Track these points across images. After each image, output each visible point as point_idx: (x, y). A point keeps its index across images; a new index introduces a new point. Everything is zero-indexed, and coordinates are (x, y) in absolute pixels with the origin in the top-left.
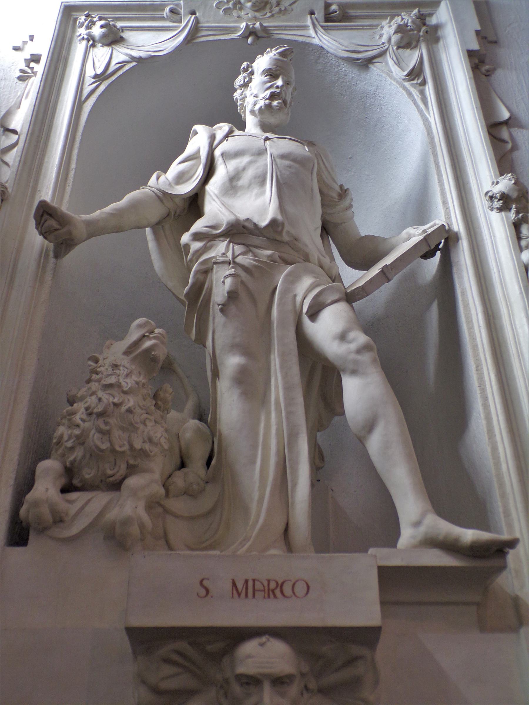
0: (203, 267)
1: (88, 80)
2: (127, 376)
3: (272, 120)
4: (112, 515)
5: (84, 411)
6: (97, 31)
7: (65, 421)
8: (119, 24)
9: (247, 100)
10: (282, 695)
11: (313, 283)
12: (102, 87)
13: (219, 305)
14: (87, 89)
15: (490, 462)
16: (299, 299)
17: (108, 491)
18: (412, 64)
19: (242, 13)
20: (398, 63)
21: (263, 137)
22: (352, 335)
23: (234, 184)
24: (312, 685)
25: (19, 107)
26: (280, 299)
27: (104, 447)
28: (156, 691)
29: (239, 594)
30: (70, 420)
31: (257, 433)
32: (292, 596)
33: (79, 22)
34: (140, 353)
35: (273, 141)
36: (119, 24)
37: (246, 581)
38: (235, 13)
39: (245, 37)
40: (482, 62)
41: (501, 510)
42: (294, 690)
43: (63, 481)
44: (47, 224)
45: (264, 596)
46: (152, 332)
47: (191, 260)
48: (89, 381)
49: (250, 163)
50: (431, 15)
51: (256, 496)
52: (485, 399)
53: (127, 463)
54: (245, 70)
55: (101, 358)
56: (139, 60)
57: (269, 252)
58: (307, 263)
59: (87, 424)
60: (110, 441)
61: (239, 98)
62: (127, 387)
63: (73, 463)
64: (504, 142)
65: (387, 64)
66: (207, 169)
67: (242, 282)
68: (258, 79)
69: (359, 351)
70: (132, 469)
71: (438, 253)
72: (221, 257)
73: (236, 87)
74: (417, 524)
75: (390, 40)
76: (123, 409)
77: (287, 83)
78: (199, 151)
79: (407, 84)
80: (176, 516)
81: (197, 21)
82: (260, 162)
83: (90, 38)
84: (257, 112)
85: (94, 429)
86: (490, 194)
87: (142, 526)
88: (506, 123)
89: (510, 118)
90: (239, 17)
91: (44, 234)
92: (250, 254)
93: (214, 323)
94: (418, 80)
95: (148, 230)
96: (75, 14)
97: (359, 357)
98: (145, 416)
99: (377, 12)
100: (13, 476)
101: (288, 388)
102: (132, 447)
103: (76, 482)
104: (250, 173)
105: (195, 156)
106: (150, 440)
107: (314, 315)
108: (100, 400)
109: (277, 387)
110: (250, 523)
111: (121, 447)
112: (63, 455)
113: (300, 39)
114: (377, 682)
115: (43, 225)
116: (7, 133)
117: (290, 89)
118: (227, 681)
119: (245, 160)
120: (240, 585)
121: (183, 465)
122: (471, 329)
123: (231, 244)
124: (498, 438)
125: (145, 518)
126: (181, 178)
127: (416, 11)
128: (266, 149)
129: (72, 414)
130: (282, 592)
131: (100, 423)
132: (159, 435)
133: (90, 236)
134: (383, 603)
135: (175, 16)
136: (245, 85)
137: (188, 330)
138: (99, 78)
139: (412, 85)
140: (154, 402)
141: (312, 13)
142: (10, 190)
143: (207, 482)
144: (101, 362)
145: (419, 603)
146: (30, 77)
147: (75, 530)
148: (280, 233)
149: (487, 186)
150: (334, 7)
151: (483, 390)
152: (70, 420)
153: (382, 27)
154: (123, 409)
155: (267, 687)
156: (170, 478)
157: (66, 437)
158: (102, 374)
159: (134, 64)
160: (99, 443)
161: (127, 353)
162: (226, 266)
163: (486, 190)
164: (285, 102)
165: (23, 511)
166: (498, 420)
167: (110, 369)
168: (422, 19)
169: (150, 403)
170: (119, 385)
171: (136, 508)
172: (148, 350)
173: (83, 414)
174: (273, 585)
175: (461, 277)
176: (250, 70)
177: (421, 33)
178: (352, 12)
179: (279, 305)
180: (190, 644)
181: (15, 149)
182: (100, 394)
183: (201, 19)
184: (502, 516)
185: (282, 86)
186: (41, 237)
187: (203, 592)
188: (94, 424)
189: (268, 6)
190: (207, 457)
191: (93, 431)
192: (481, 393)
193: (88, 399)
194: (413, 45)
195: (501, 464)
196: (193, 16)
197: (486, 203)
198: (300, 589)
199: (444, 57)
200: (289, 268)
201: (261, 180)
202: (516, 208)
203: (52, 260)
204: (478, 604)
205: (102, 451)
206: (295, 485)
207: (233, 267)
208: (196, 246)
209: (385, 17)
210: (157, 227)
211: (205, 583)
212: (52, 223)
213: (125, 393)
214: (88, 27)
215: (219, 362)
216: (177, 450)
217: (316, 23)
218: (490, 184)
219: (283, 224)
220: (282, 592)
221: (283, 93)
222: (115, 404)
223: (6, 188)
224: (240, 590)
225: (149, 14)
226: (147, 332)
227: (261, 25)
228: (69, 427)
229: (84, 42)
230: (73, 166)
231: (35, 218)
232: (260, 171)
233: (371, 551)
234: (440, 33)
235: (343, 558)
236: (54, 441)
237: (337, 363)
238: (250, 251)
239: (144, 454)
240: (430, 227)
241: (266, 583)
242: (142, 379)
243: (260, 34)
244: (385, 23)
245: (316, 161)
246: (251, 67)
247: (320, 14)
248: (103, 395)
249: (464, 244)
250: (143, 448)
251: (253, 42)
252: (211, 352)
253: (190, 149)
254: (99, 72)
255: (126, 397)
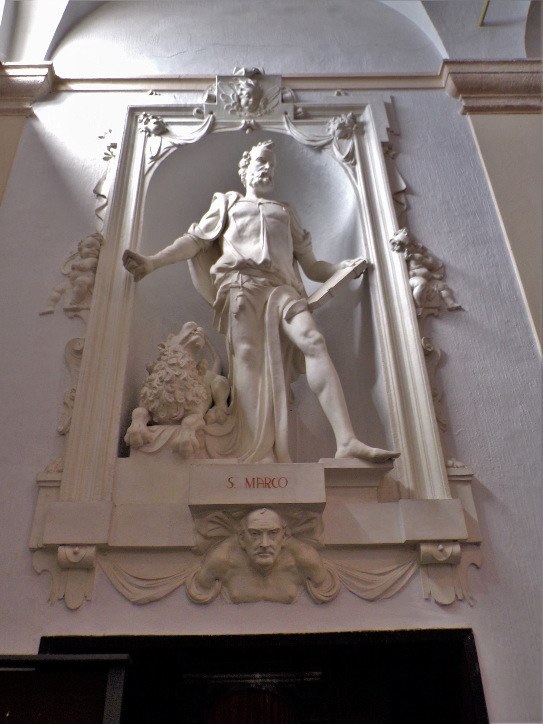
0: (225, 290)
1: (148, 160)
2: (182, 358)
3: (262, 190)
4: (177, 439)
5: (158, 379)
6: (152, 126)
7: (147, 384)
8: (166, 120)
9: (247, 176)
10: (273, 539)
11: (288, 299)
12: (157, 165)
13: (234, 313)
14: (147, 166)
15: (387, 407)
16: (280, 309)
17: (174, 425)
18: (348, 150)
19: (242, 113)
20: (340, 149)
21: (258, 203)
22: (312, 333)
23: (241, 234)
24: (289, 532)
25: (105, 179)
26: (270, 310)
27: (171, 401)
28: (206, 537)
29: (250, 486)
30: (150, 384)
31: (257, 390)
32: (278, 487)
33: (140, 120)
34: (188, 344)
35: (264, 206)
36: (166, 120)
37: (254, 479)
38: (238, 113)
39: (244, 129)
40: (390, 148)
41: (392, 434)
42: (279, 537)
43: (148, 420)
44: (131, 264)
45: (263, 487)
46: (195, 330)
47: (217, 284)
48: (159, 359)
49: (251, 221)
50: (359, 115)
51: (257, 426)
52: (386, 369)
53: (184, 409)
54: (246, 157)
55: (166, 345)
56: (179, 146)
57: (263, 279)
58: (285, 285)
59: (161, 387)
60: (174, 397)
61: (242, 175)
62: (183, 365)
63: (153, 409)
64: (402, 204)
65: (333, 150)
66: (224, 223)
67: (248, 299)
68: (254, 163)
69: (315, 343)
70: (187, 413)
71: (362, 276)
72: (235, 283)
73: (241, 167)
74: (346, 445)
75: (334, 133)
76: (182, 378)
77: (271, 166)
78: (218, 211)
79: (345, 164)
80: (211, 435)
81: (214, 118)
82: (256, 221)
83: (147, 130)
84: (253, 185)
85: (165, 390)
86: (393, 241)
87: (194, 445)
88: (404, 191)
89: (406, 189)
90: (240, 116)
91: (129, 269)
92: (252, 281)
93: (231, 324)
94: (351, 161)
95: (189, 261)
96: (137, 113)
97: (315, 347)
98: (193, 381)
99: (326, 113)
100: (119, 417)
101: (275, 364)
102: (187, 400)
103: (155, 420)
104: (250, 228)
105: (216, 214)
106: (197, 395)
107: (289, 319)
108: (168, 373)
109: (268, 362)
110: (254, 443)
111: (180, 400)
112: (147, 404)
113: (279, 131)
114: (323, 530)
115: (128, 264)
116: (99, 197)
117: (274, 169)
118: (243, 532)
119: (247, 219)
120: (250, 481)
121: (213, 404)
122: (379, 326)
123: (240, 275)
124: (392, 392)
125: (196, 441)
126: (209, 228)
127: (350, 114)
128: (259, 211)
129: (151, 380)
130: (273, 484)
131: (169, 387)
132: (201, 392)
133: (156, 268)
134: (327, 487)
135: (200, 115)
136: (246, 166)
137: (215, 325)
138: (154, 159)
139: (348, 165)
140: (198, 372)
141: (286, 113)
142: (105, 238)
143: (228, 415)
144: (166, 348)
145: (346, 487)
146: (110, 158)
147: (155, 448)
148: (269, 268)
149: (391, 236)
150: (300, 110)
151: (385, 363)
152: (150, 384)
153: (330, 124)
154: (182, 378)
155: (265, 535)
156: (207, 414)
157: (148, 394)
158: (168, 356)
159: (175, 148)
160: (168, 399)
161: (182, 343)
162: (237, 290)
163: (390, 238)
164: (270, 179)
165: (126, 438)
166: (393, 381)
167: (172, 354)
168: (354, 119)
169: (196, 372)
170: (178, 364)
171: (190, 435)
172: (194, 342)
173: (158, 381)
174: (268, 481)
175: (374, 294)
176: (249, 157)
177: (354, 129)
178: (311, 113)
179: (269, 313)
180: (224, 512)
181: (106, 209)
182: (168, 369)
183: (217, 117)
184: (393, 437)
185: (269, 169)
186: (127, 270)
187: (230, 485)
188: (164, 387)
189: (258, 109)
190: (227, 397)
191: (164, 391)
192: (384, 365)
193: (160, 372)
194: (349, 136)
195: (393, 408)
196: (212, 116)
197: (391, 246)
198: (283, 483)
199: (367, 145)
200: (275, 289)
201: (257, 232)
202: (408, 250)
203: (133, 283)
204: (378, 487)
205: (170, 403)
206: (279, 420)
207: (242, 290)
208: (220, 275)
209: (330, 116)
210: (194, 259)
211: (231, 480)
212: (134, 263)
213: (182, 368)
214: (146, 123)
215: (234, 346)
216: (210, 395)
217: (288, 120)
218: (393, 234)
219: (271, 262)
220: (273, 484)
221: (269, 172)
222: (176, 376)
223: (102, 237)
224: (250, 484)
225: (183, 113)
226: (193, 331)
227: (254, 122)
228: (150, 388)
229: (144, 133)
230: (142, 219)
231: (123, 260)
232: (256, 226)
233: (321, 461)
234: (365, 128)
235: (306, 465)
236: (142, 396)
237: (303, 349)
238: (252, 278)
239: (193, 403)
240: (357, 261)
241: (264, 480)
242: (191, 359)
243: (254, 128)
244: (331, 120)
245: (290, 218)
246: (250, 155)
247: (291, 114)
248: (169, 370)
249: (377, 272)
250: (193, 400)
251: (250, 133)
252: (230, 340)
253: (213, 209)
254: (154, 155)
255: (183, 370)
